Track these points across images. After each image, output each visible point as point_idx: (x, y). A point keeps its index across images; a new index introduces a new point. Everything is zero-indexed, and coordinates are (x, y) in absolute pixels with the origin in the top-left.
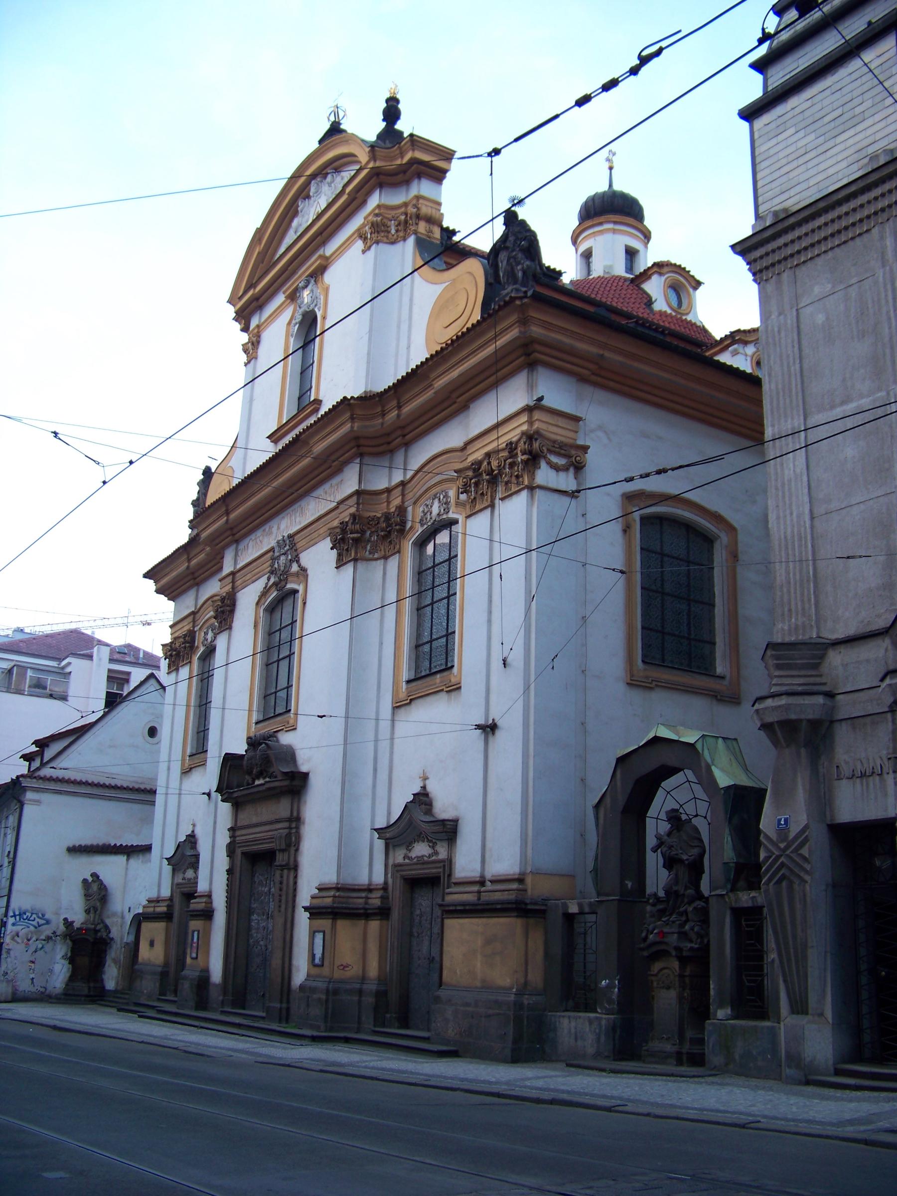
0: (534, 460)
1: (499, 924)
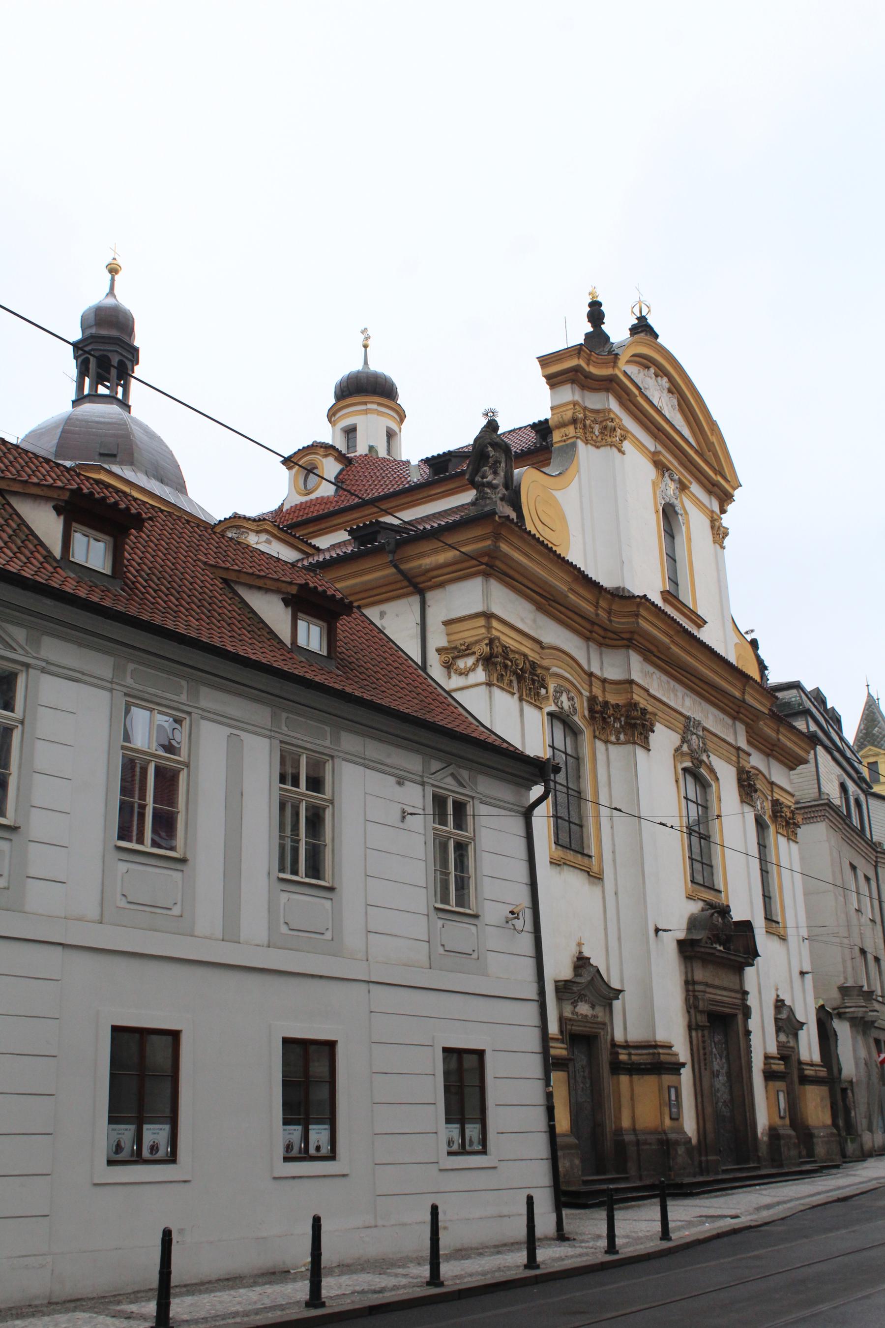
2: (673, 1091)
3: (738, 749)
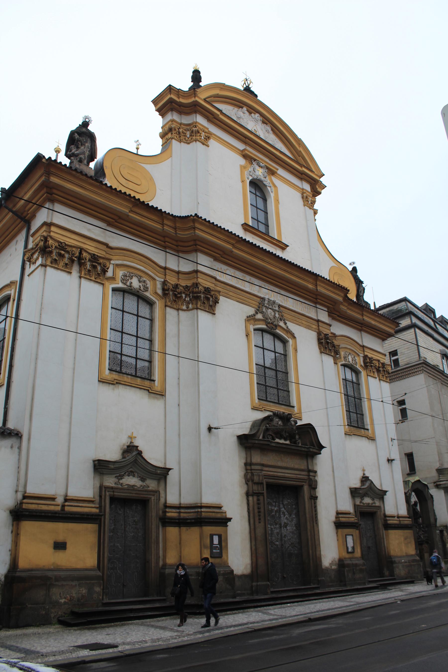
3: (318, 321)
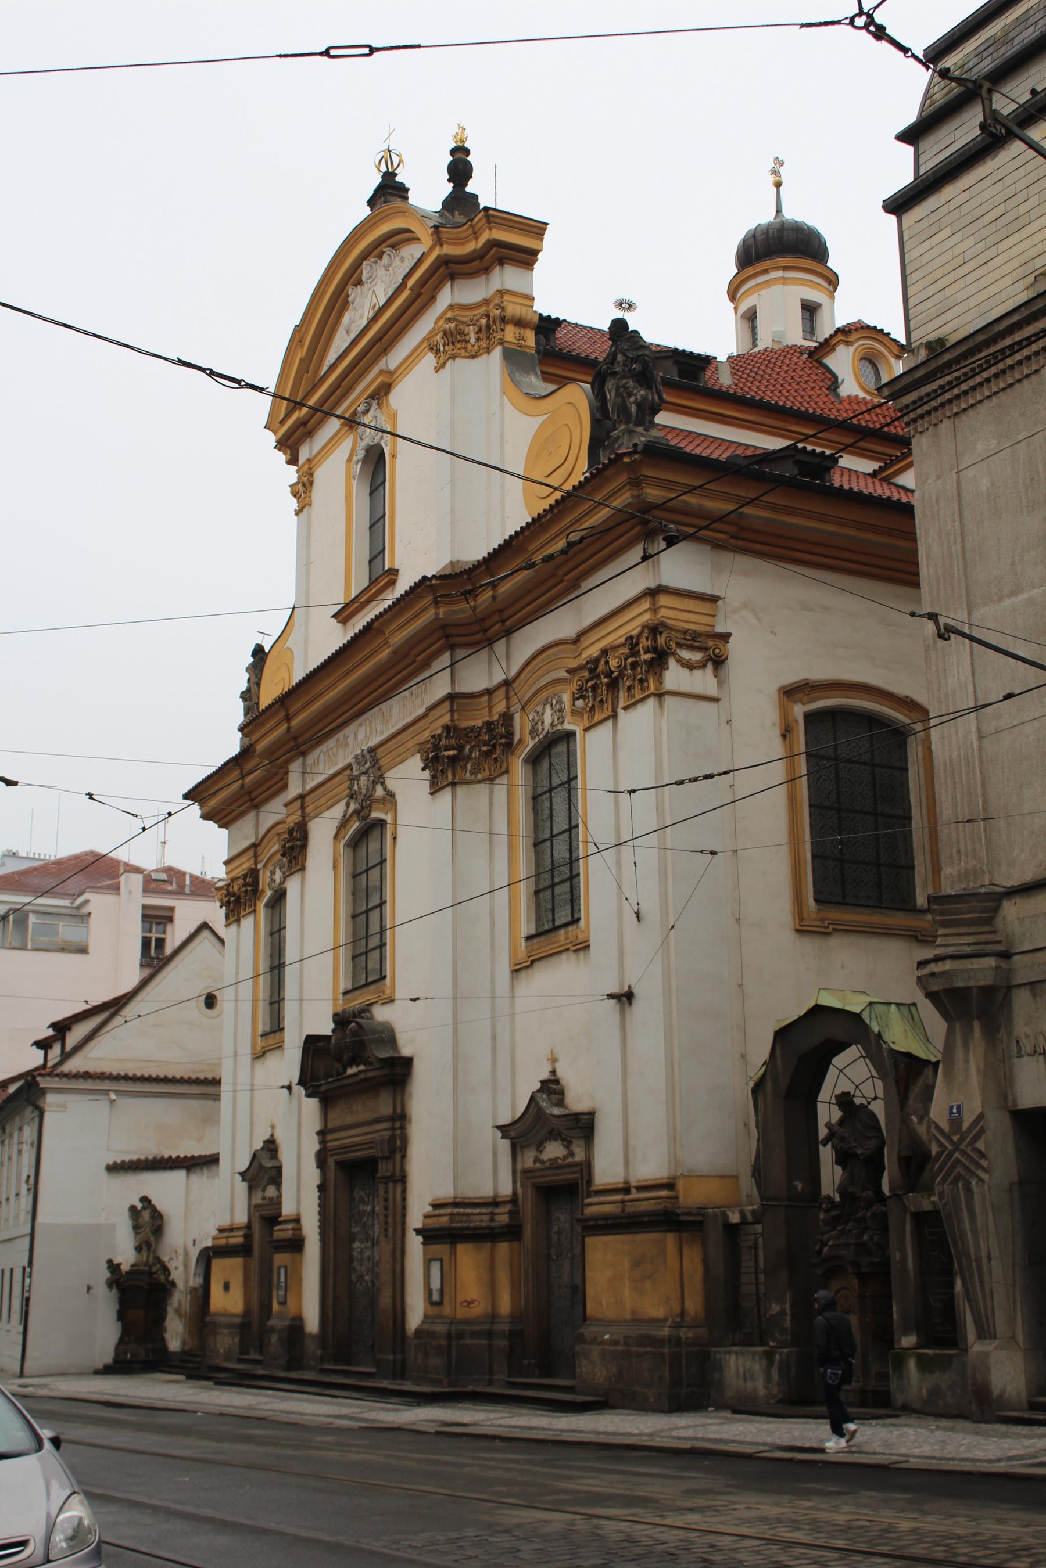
0: (660, 659)
1: (645, 1240)
2: (282, 1271)
